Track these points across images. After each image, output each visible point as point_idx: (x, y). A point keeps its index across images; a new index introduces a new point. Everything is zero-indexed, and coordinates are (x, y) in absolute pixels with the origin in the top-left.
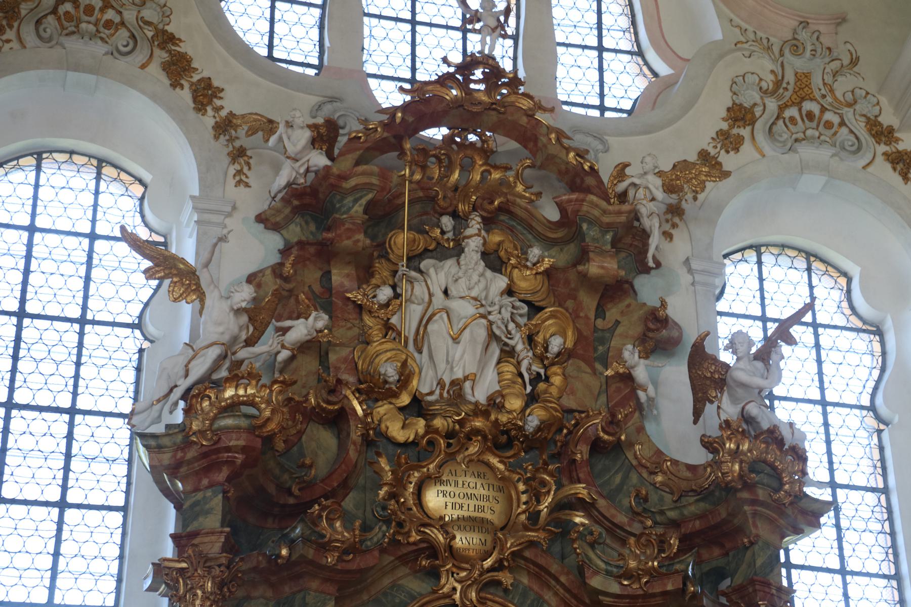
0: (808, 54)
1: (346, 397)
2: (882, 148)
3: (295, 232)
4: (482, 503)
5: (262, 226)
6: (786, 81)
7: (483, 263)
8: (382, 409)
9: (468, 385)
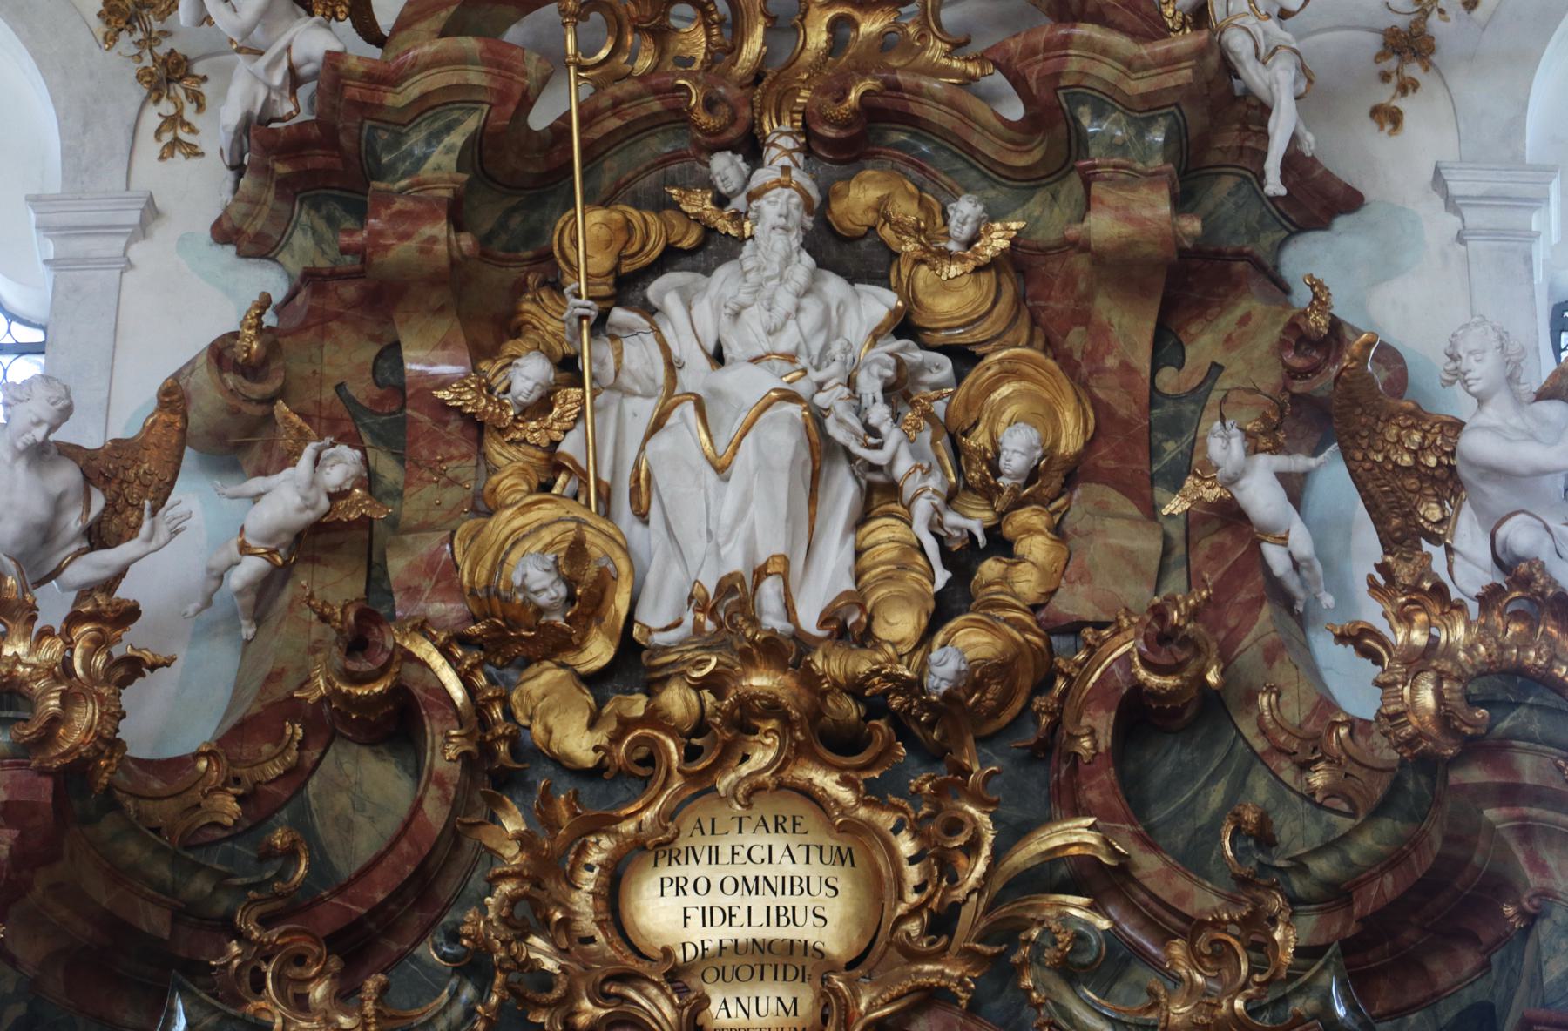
3: (303, 248)
4: (787, 901)
5: (231, 250)
7: (807, 260)
8: (544, 679)
9: (770, 590)
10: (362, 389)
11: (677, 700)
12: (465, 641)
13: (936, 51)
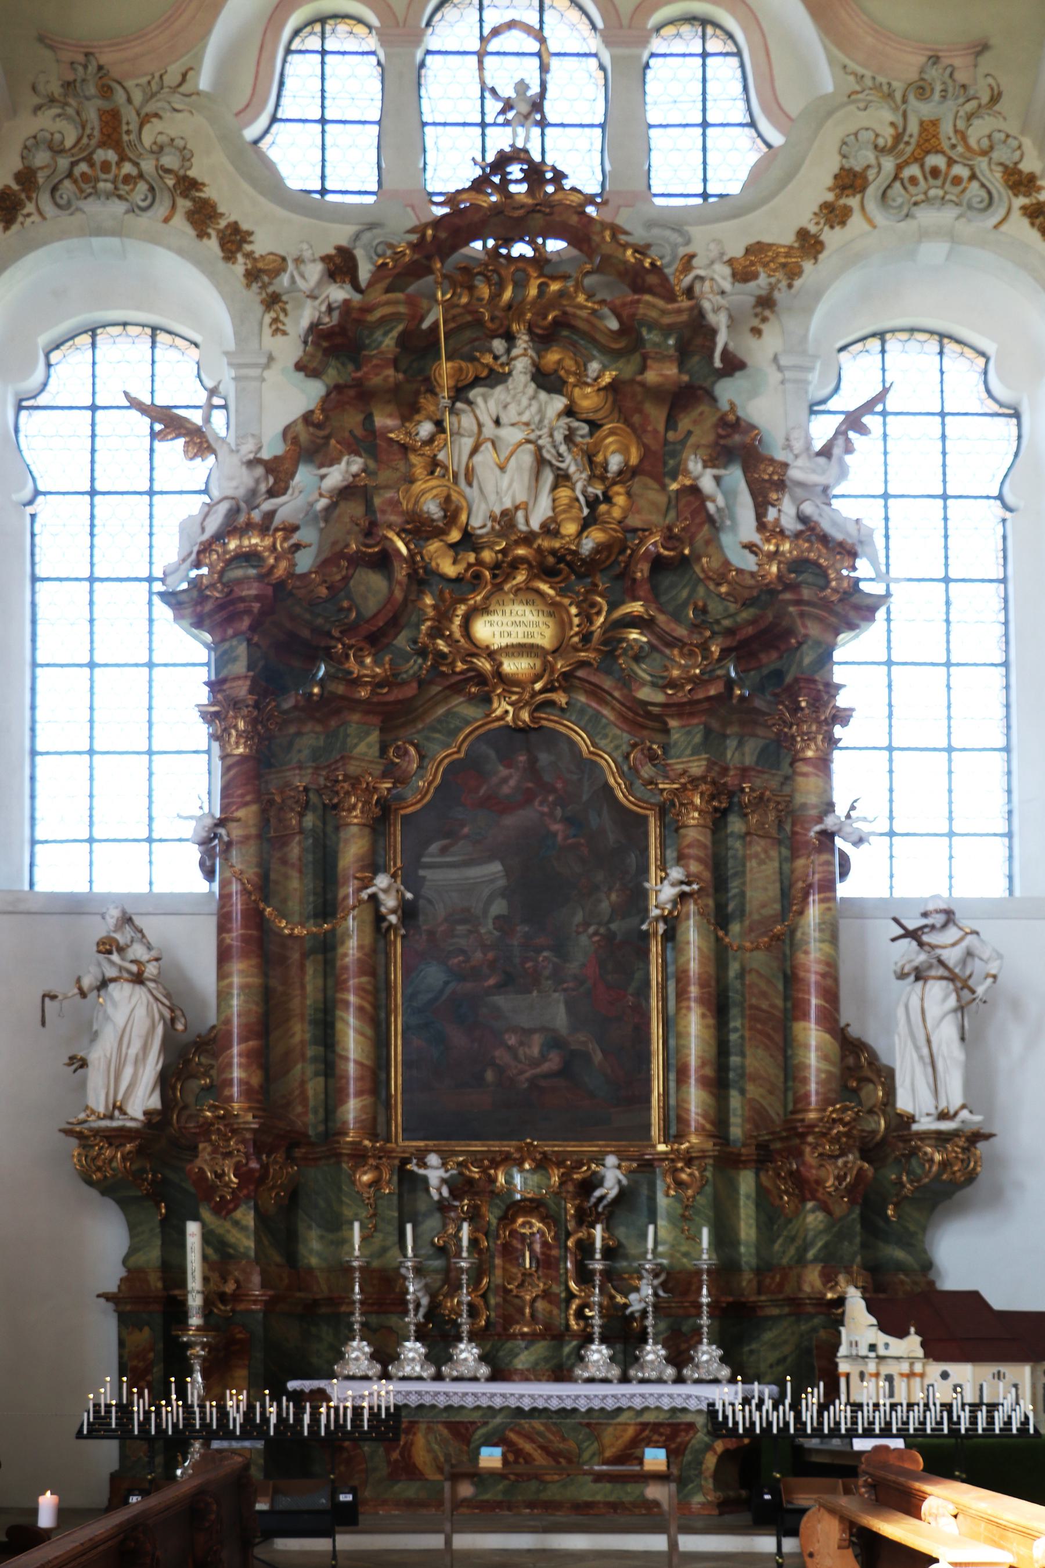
0: (937, 95)
1: (386, 538)
3: (332, 375)
6: (908, 132)
7: (533, 386)
9: (520, 515)
10: (359, 432)
11: (487, 555)
12: (404, 530)
13: (581, 298)
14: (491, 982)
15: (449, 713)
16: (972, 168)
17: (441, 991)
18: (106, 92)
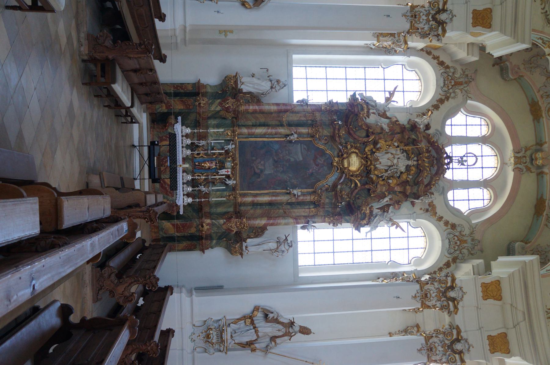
0: (472, 243)
2: (451, 260)
8: (372, 146)
14: (275, 158)
15: (335, 149)
16: (457, 250)
17: (273, 148)
18: (466, 83)
